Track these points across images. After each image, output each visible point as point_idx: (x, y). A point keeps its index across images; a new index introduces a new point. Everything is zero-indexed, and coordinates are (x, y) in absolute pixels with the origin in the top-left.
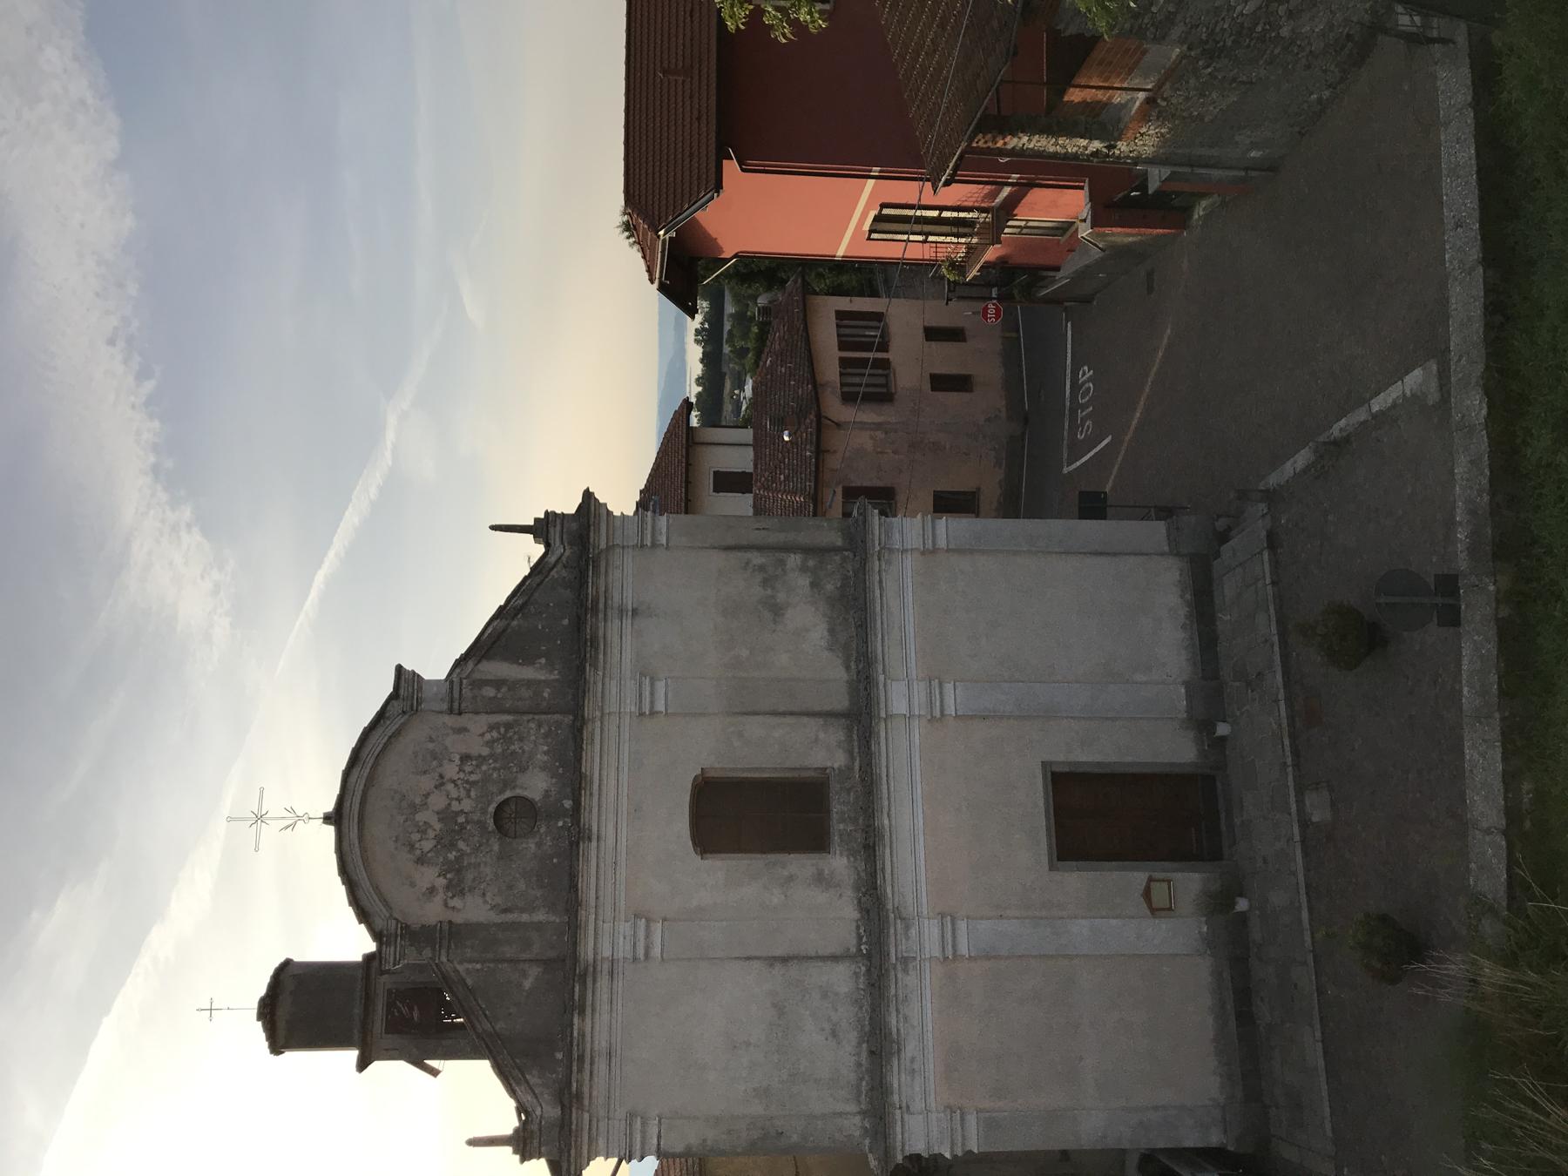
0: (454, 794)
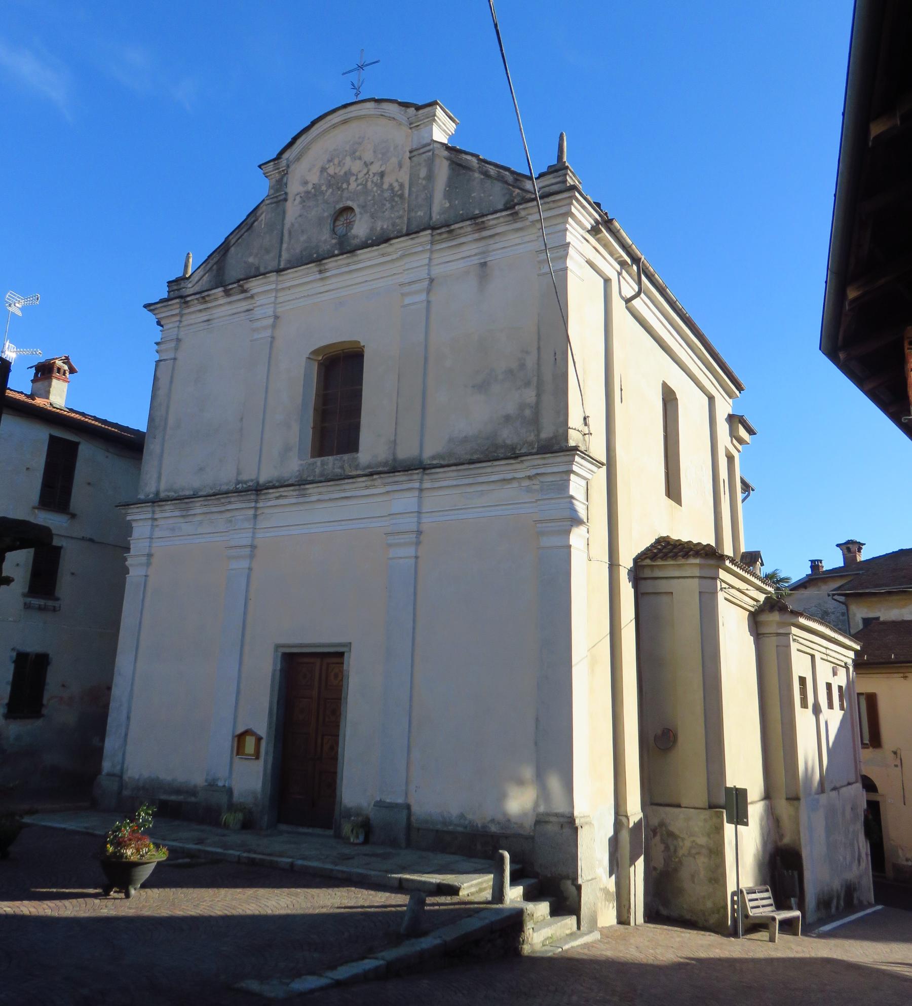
0: (360, 176)
